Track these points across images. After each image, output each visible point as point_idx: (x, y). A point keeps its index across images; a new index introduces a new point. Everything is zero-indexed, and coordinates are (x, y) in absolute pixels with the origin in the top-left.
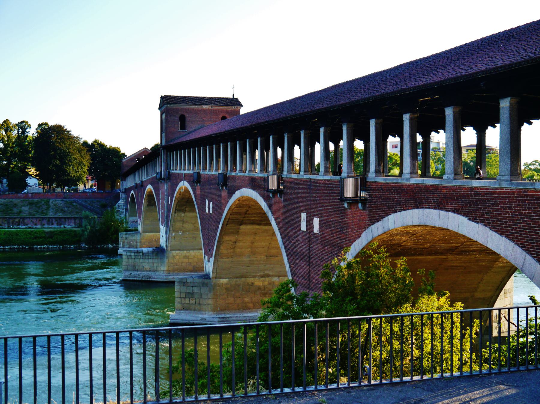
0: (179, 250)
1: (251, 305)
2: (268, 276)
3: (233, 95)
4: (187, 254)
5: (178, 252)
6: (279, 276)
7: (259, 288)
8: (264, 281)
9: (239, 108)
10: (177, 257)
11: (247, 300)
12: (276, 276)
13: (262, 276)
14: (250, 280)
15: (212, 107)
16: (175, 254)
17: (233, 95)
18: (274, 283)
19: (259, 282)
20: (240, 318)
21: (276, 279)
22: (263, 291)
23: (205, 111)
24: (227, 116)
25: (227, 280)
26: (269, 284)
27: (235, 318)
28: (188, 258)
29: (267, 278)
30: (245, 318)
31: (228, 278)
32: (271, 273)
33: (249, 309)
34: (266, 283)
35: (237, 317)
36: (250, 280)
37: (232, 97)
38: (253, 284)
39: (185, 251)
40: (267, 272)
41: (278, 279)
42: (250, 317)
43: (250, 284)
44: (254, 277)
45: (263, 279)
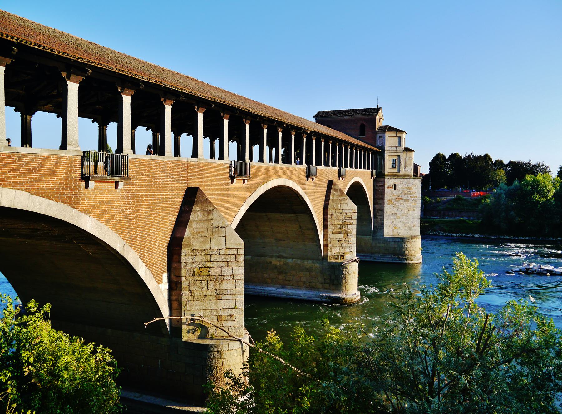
1: (269, 280)
2: (283, 257)
3: (378, 105)
6: (293, 258)
7: (276, 267)
8: (280, 261)
9: (375, 116)
11: (266, 275)
12: (290, 258)
13: (278, 257)
14: (269, 259)
15: (351, 117)
17: (378, 105)
18: (288, 263)
19: (276, 262)
20: (257, 290)
21: (290, 260)
22: (279, 270)
23: (346, 120)
25: (250, 257)
26: (285, 264)
27: (252, 290)
29: (282, 259)
30: (261, 291)
31: (251, 256)
32: (285, 255)
33: (268, 283)
34: (282, 263)
35: (254, 289)
36: (269, 259)
38: (271, 262)
40: (281, 254)
41: (292, 260)
42: (265, 290)
43: (268, 262)
44: (272, 257)
45: (279, 259)
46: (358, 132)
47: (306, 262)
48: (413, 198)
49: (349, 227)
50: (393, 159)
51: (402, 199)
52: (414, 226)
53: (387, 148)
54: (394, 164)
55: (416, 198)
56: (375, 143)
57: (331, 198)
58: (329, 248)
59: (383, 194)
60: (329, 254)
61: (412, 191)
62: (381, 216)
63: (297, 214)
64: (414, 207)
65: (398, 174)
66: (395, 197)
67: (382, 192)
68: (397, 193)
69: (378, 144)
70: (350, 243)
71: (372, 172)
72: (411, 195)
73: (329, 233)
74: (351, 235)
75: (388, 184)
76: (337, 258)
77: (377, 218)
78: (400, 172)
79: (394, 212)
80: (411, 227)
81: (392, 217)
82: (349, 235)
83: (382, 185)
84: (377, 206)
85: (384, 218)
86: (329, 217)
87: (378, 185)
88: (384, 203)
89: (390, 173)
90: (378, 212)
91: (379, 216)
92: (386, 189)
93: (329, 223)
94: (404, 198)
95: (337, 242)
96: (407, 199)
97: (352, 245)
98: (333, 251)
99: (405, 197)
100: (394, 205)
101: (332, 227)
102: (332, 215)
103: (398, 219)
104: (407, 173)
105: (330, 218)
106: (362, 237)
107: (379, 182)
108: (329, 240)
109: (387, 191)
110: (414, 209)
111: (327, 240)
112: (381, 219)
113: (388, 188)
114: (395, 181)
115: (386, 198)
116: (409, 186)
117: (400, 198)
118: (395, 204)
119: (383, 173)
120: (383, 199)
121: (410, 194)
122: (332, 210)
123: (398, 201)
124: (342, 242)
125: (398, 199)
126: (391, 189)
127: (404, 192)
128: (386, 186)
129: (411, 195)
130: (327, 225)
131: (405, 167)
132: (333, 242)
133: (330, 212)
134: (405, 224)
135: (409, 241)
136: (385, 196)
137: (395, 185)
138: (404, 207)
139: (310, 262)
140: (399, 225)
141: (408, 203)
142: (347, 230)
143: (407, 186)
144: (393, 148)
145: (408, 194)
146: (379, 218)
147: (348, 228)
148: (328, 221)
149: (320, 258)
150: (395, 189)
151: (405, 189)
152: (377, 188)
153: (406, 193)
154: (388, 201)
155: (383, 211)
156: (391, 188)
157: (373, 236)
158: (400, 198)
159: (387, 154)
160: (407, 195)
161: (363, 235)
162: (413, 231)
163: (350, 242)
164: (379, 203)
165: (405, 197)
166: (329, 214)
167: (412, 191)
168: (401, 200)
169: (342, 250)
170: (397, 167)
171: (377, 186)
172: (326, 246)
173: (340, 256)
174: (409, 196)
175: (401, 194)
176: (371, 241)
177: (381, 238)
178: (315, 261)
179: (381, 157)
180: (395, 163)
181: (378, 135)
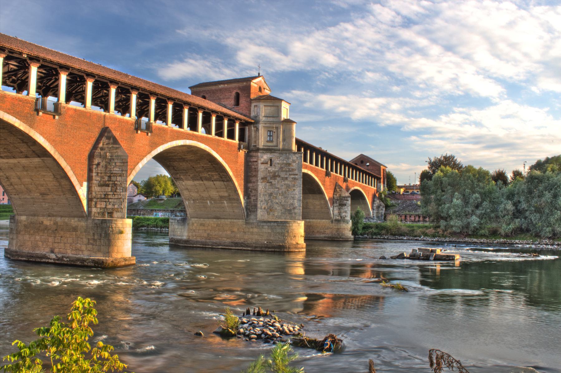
0: (197, 218)
3: (259, 74)
4: (203, 222)
5: (196, 219)
10: (195, 225)
16: (194, 222)
17: (259, 74)
21: (59, 219)
24: (239, 91)
28: (204, 226)
31: (26, 215)
36: (41, 219)
37: (257, 75)
38: (42, 222)
39: (202, 219)
43: (40, 222)
46: (232, 102)
47: (73, 221)
48: (292, 176)
49: (119, 178)
50: (270, 131)
51: (279, 176)
52: (294, 208)
53: (262, 118)
54: (271, 137)
55: (297, 177)
56: (250, 114)
57: (101, 145)
58: (94, 203)
59: (256, 170)
60: (94, 210)
61: (291, 167)
62: (255, 196)
63: (42, 158)
64: (294, 186)
65: (276, 148)
66: (271, 174)
67: (256, 168)
68: (274, 169)
69: (253, 114)
70: (120, 198)
71: (240, 145)
72: (291, 173)
73: (93, 185)
74: (122, 188)
75: (262, 160)
76: (103, 214)
77: (250, 198)
78: (277, 146)
79: (269, 192)
80: (290, 210)
81: (267, 198)
82: (118, 188)
83: (255, 160)
84: (250, 185)
85: (257, 199)
86: (94, 166)
87: (252, 160)
88: (257, 181)
89: (265, 147)
90: (251, 191)
91: (252, 196)
92: (260, 165)
93: (94, 174)
94: (283, 176)
95: (103, 196)
96: (286, 176)
97: (122, 200)
98: (98, 206)
99: (283, 175)
100: (269, 184)
101: (98, 179)
102: (98, 164)
103: (274, 201)
104: (286, 148)
105: (96, 168)
106: (235, 221)
107: (251, 156)
108: (94, 193)
109: (261, 167)
110: (294, 188)
111: (91, 193)
112: (254, 199)
113: (262, 163)
114: (271, 156)
115: (260, 175)
116: (288, 162)
117: (277, 176)
118: (271, 182)
119: (257, 147)
120: (256, 176)
121: (290, 171)
122: (99, 159)
123: (275, 179)
124: (109, 197)
125: (274, 176)
126: (266, 165)
127: (281, 168)
128: (260, 162)
129: (291, 173)
130: (92, 176)
131: (284, 140)
132: (99, 196)
133: (96, 161)
134: (283, 205)
135: (284, 225)
136: (259, 173)
137: (271, 160)
138: (282, 186)
139: (76, 219)
140: (276, 206)
141: (286, 182)
142: (116, 182)
143: (285, 162)
144: (269, 118)
145: (286, 171)
146: (253, 198)
147: (118, 180)
148: (94, 171)
149: (85, 215)
150: (271, 165)
151: (283, 166)
152: (250, 164)
153: (284, 169)
154: (262, 179)
155: (256, 190)
156: (267, 163)
157: (246, 220)
158: (277, 176)
159: (261, 126)
160: (285, 173)
161: (235, 219)
162: (293, 215)
163: (120, 197)
164: (253, 181)
165: (283, 175)
166: (94, 163)
167: (291, 167)
168: (278, 179)
169: (110, 206)
170: (274, 140)
171: (251, 162)
172: (89, 200)
173: (106, 215)
174: (288, 174)
175: (278, 171)
176: (244, 226)
177: (255, 221)
178: (80, 219)
179: (255, 128)
180: (272, 136)
181: (253, 105)
